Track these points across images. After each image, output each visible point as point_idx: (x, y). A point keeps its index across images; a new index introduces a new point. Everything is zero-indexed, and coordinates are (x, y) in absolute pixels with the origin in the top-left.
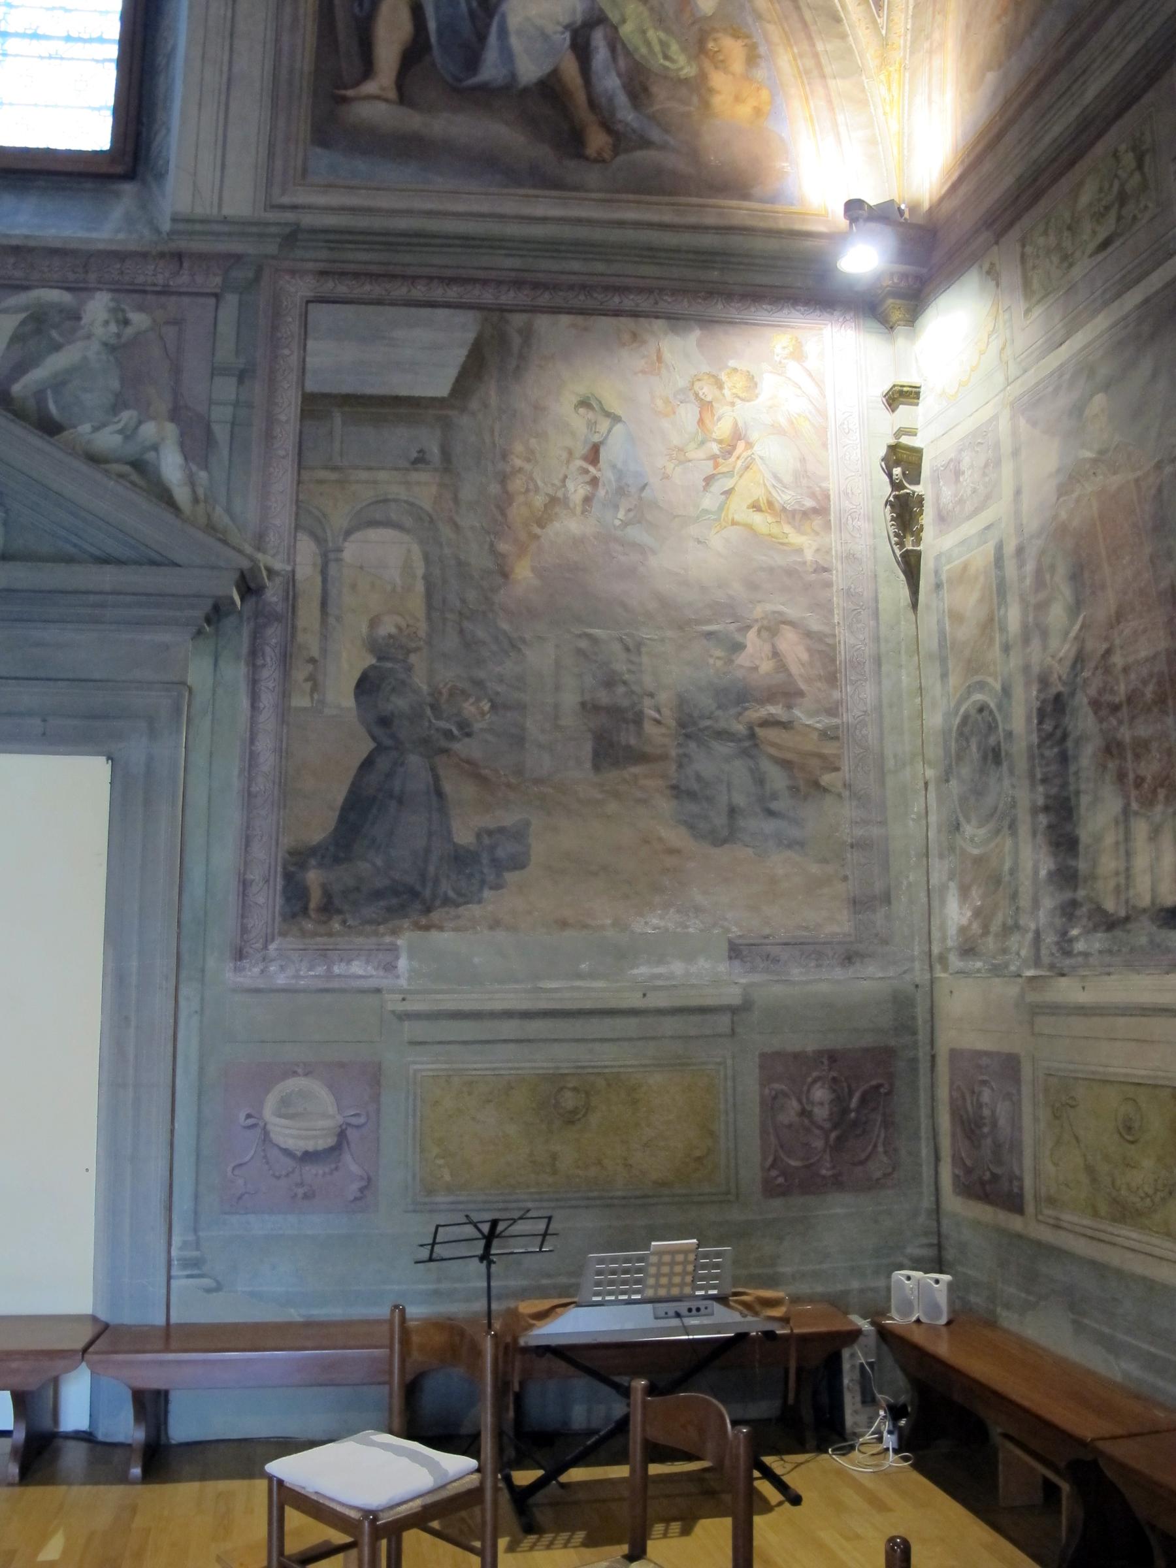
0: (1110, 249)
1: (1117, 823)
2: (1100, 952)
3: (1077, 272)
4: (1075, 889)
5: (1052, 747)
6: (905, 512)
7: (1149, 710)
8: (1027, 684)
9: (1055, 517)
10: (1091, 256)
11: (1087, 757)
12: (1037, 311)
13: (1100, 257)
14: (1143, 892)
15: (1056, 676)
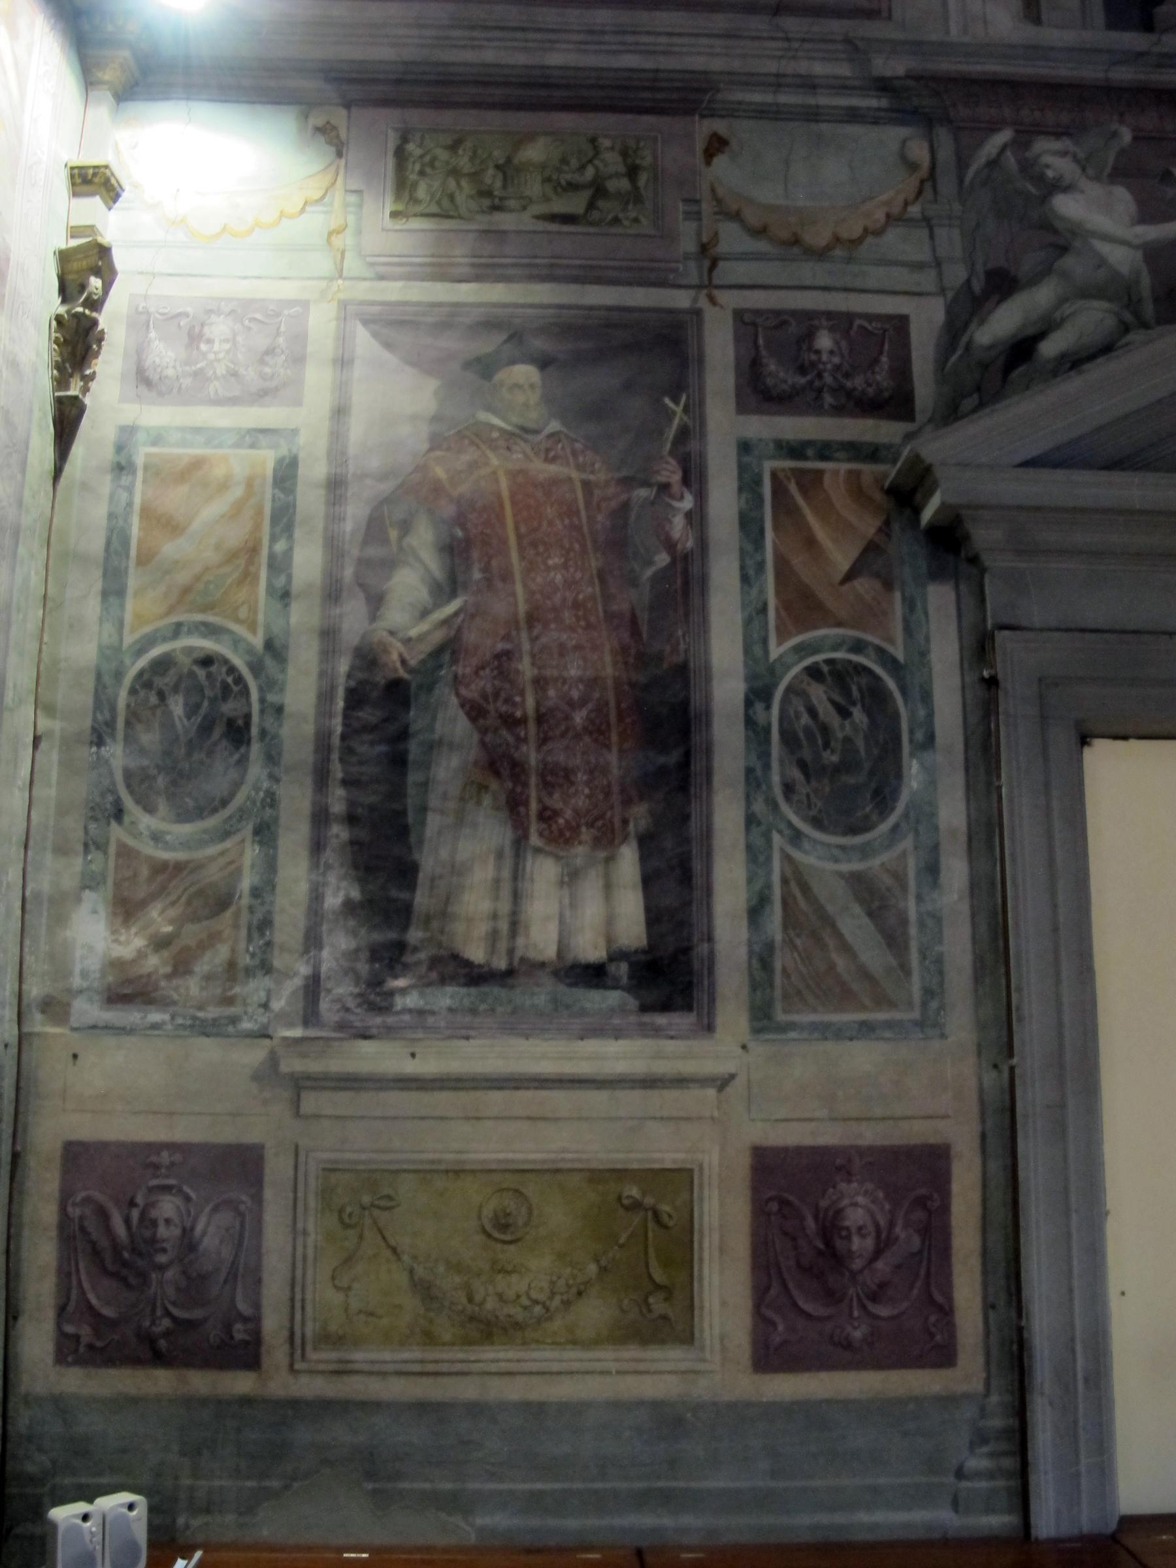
0: (566, 228)
1: (500, 855)
2: (451, 1010)
3: (506, 221)
4: (405, 927)
5: (372, 744)
6: (77, 343)
7: (578, 737)
8: (328, 652)
9: (421, 468)
10: (538, 217)
11: (447, 771)
12: (416, 224)
13: (554, 227)
14: (542, 940)
15: (395, 656)
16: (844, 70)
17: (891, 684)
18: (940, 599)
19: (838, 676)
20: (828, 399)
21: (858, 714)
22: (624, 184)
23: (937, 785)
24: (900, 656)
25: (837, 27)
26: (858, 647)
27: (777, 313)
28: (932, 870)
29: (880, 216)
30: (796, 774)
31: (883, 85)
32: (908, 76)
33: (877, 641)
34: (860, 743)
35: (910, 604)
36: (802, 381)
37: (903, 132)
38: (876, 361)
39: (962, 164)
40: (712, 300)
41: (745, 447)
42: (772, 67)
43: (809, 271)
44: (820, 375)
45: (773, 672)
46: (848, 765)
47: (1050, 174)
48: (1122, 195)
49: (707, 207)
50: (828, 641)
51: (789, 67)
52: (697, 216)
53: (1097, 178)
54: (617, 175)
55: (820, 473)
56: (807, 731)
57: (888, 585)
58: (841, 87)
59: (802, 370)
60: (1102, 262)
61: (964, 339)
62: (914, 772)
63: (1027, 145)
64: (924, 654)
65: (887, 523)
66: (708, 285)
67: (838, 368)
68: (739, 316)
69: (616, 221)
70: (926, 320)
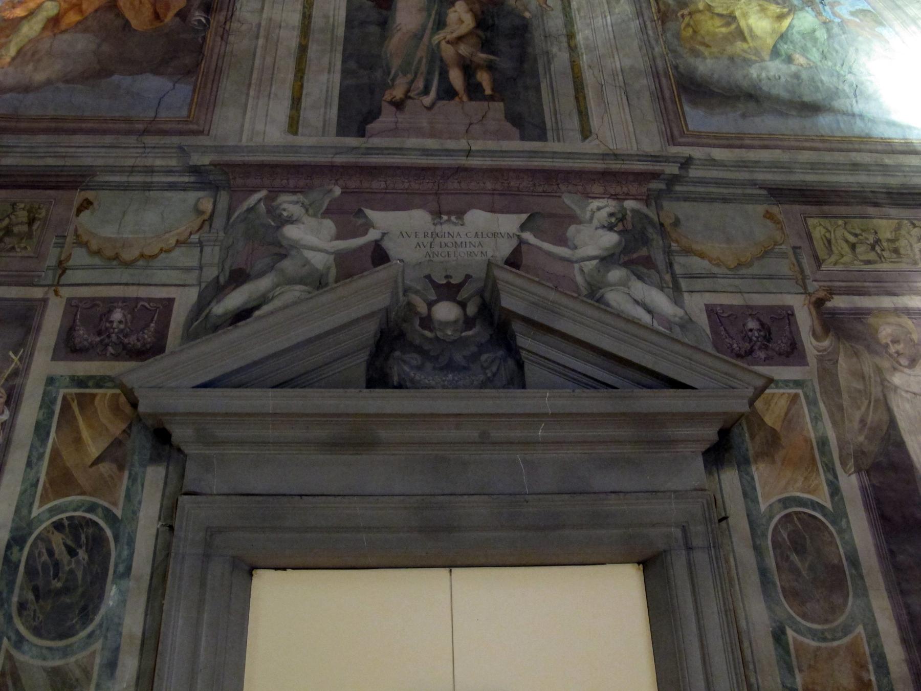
16: (173, 162)
17: (109, 533)
18: (154, 476)
19: (73, 528)
20: (110, 349)
21: (82, 554)
22: (25, 228)
23: (124, 605)
24: (118, 512)
25: (176, 140)
26: (92, 508)
27: (93, 299)
28: (111, 666)
29: (173, 241)
30: (31, 596)
31: (195, 170)
32: (211, 164)
33: (106, 504)
34: (80, 574)
35: (133, 479)
36: (98, 339)
37: (200, 194)
38: (148, 326)
39: (231, 210)
40: (56, 293)
41: (51, 381)
42: (130, 162)
43: (125, 275)
44: (109, 336)
45: (31, 525)
46: (66, 590)
47: (285, 214)
48: (329, 226)
49: (70, 239)
50: (71, 505)
51: (140, 162)
52: (61, 245)
53: (315, 215)
54: (22, 223)
55: (94, 396)
56: (44, 565)
57: (121, 468)
58: (169, 171)
59: (99, 333)
60: (307, 262)
61: (207, 311)
62: (112, 592)
63: (274, 199)
64: (135, 513)
65: (130, 427)
66: (56, 286)
67: (121, 331)
68: (69, 300)
69: (13, 248)
70: (185, 300)
